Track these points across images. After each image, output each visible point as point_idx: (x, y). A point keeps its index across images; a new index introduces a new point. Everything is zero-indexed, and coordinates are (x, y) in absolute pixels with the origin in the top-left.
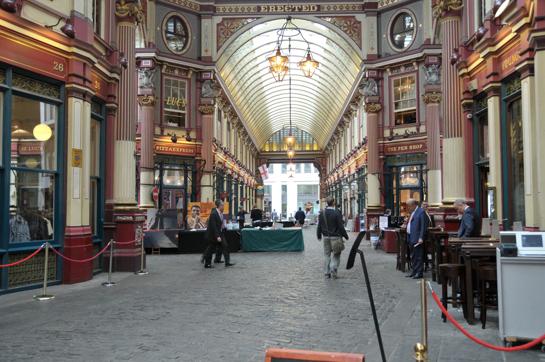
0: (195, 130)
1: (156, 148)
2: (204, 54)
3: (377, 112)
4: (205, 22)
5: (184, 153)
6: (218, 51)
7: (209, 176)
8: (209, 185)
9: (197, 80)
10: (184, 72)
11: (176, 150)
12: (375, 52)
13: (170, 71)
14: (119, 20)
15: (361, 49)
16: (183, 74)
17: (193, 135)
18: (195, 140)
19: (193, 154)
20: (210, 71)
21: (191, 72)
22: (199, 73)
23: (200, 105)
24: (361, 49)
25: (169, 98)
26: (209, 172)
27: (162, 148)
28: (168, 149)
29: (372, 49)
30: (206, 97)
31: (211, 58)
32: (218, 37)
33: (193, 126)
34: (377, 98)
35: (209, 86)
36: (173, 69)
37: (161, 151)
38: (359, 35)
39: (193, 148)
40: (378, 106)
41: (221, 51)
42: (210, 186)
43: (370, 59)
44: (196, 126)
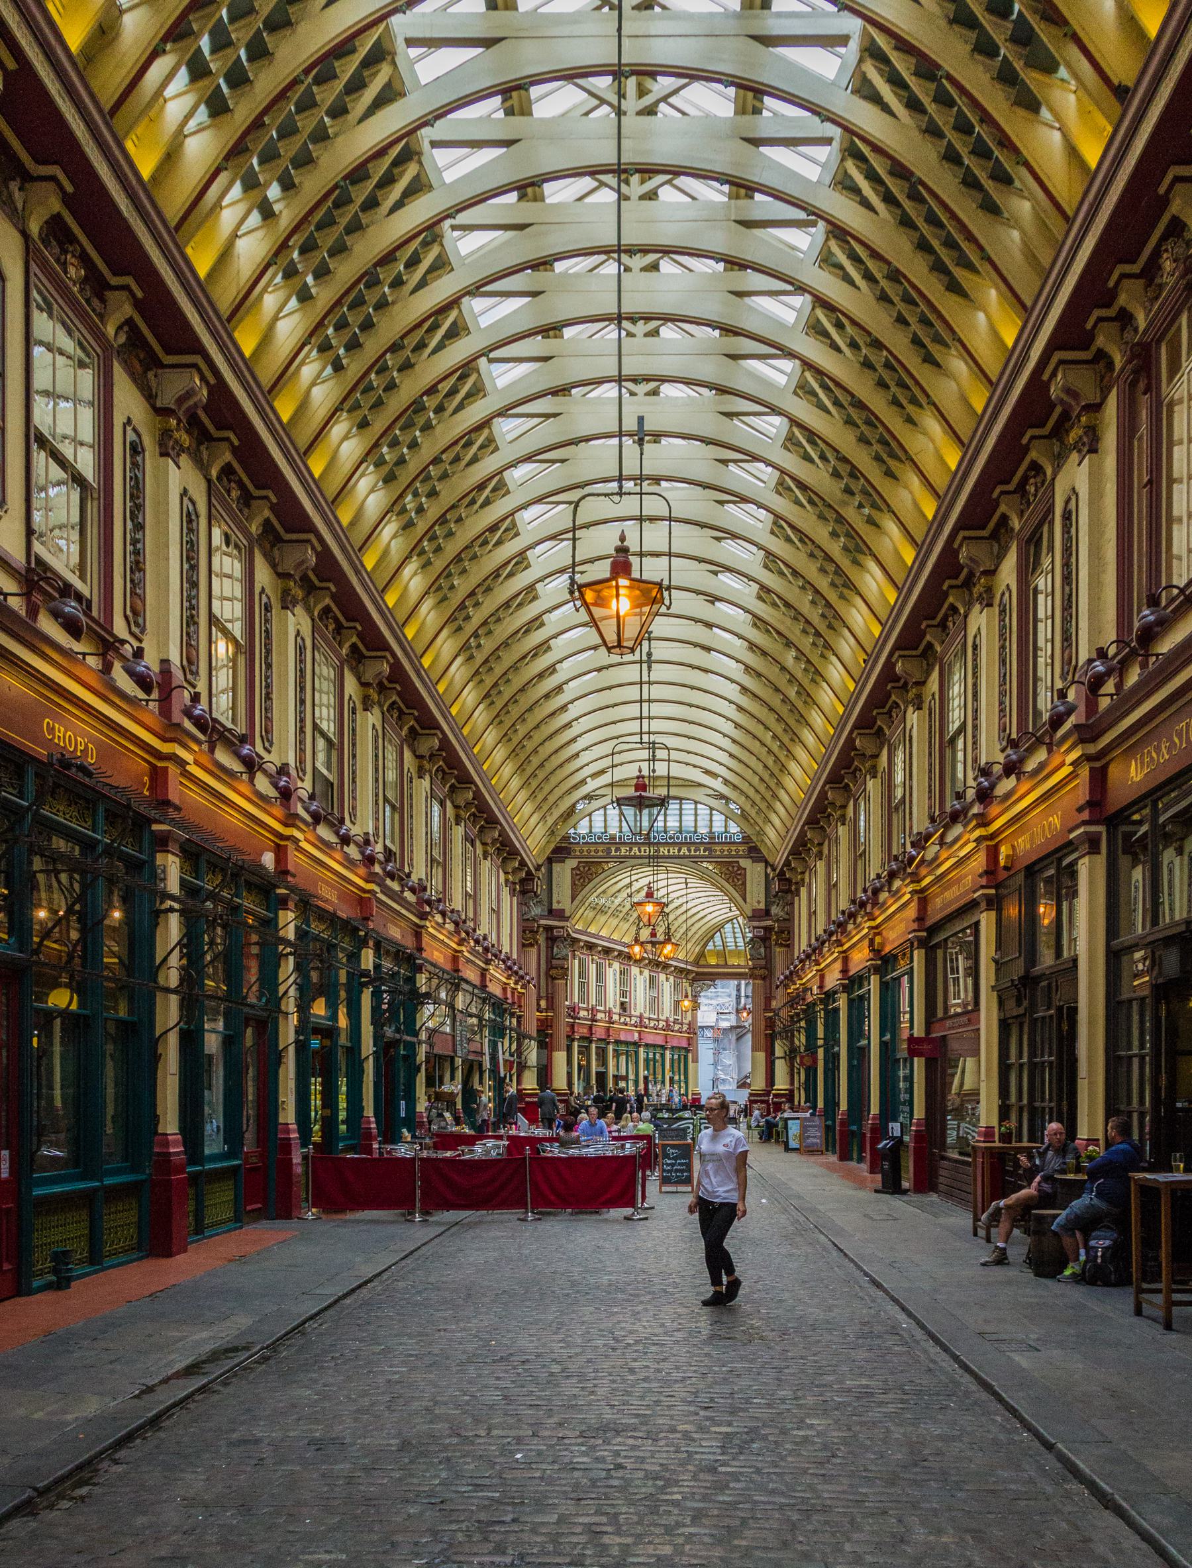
2: (555, 906)
3: (764, 978)
4: (556, 867)
9: (547, 938)
14: (524, 945)
15: (745, 900)
17: (543, 1003)
18: (546, 1010)
20: (563, 928)
22: (549, 929)
23: (552, 968)
24: (745, 900)
29: (759, 902)
32: (573, 884)
33: (543, 994)
34: (763, 962)
38: (744, 884)
40: (762, 972)
41: (576, 902)
43: (756, 915)
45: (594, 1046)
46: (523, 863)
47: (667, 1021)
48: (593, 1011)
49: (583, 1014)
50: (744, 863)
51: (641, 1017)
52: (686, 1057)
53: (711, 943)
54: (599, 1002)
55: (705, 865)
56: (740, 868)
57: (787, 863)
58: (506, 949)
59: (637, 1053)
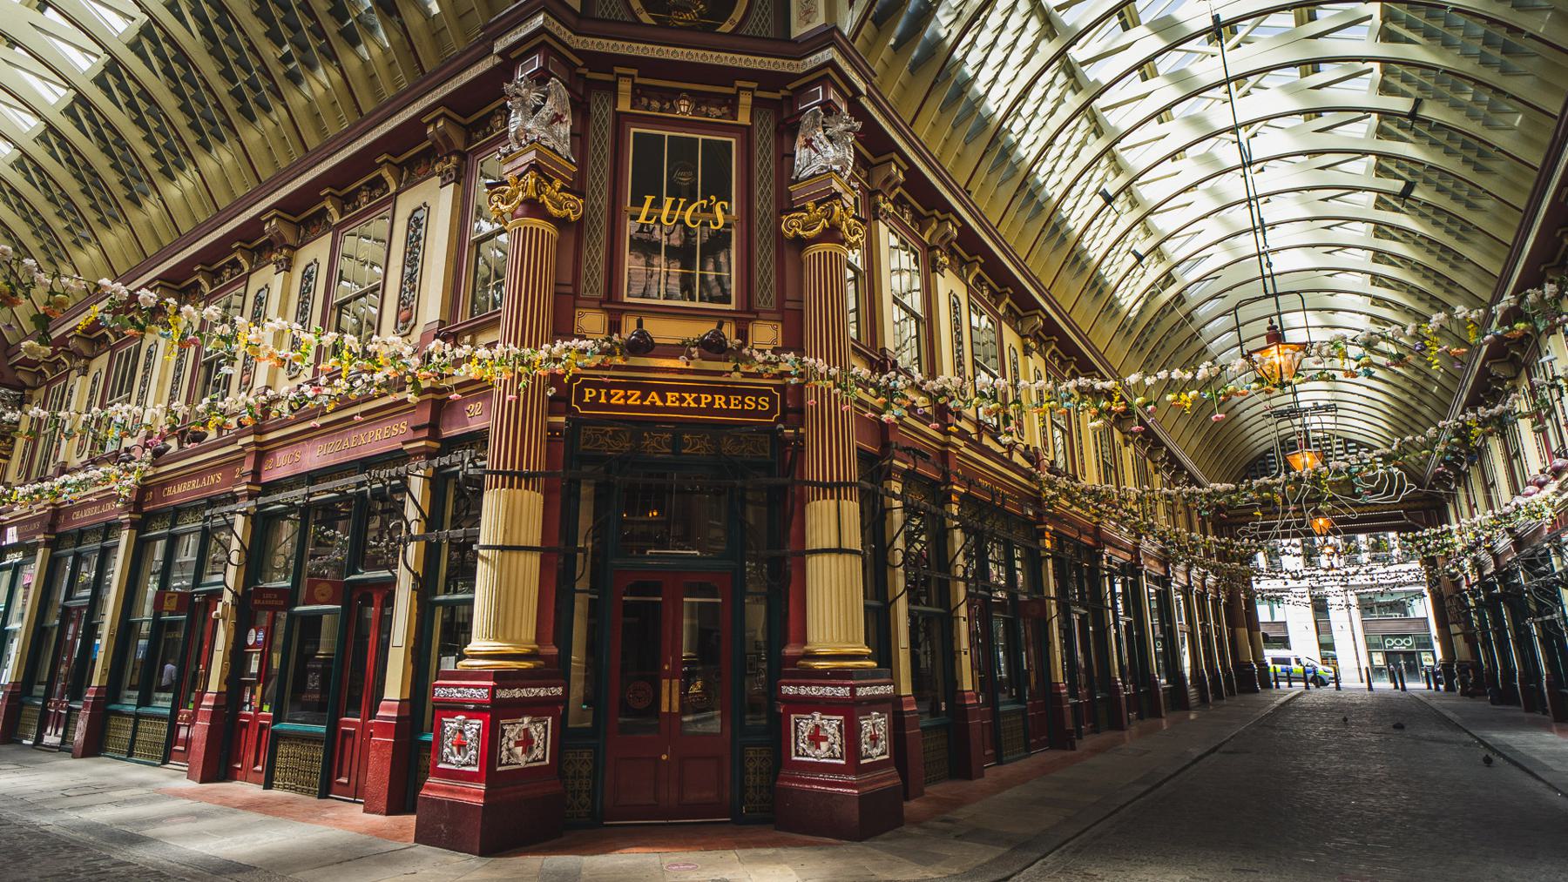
0: (777, 316)
1: (581, 395)
5: (720, 412)
7: (833, 503)
8: (834, 545)
10: (719, 107)
11: (682, 400)
13: (656, 104)
16: (718, 113)
19: (769, 414)
21: (745, 100)
25: (649, 199)
26: (831, 486)
27: (609, 397)
28: (643, 397)
30: (814, 175)
33: (765, 298)
35: (820, 133)
36: (671, 96)
37: (608, 407)
39: (768, 393)
42: (840, 551)
44: (782, 298)
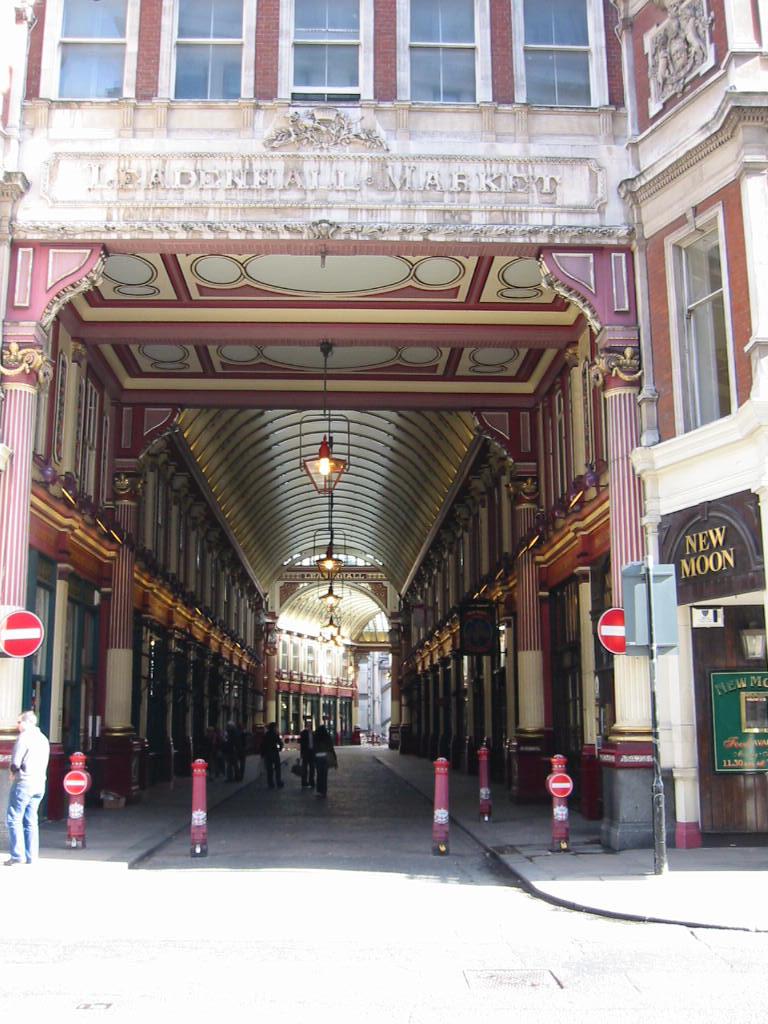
2: (270, 610)
6: (281, 605)
12: (397, 610)
31: (274, 613)
34: (397, 645)
40: (398, 651)
45: (291, 697)
46: (258, 594)
47: (338, 679)
48: (290, 674)
49: (285, 676)
50: (385, 583)
51: (321, 677)
52: (350, 704)
53: (367, 628)
54: (295, 669)
55: (363, 585)
56: (383, 587)
57: (406, 594)
58: (248, 644)
59: (318, 702)
